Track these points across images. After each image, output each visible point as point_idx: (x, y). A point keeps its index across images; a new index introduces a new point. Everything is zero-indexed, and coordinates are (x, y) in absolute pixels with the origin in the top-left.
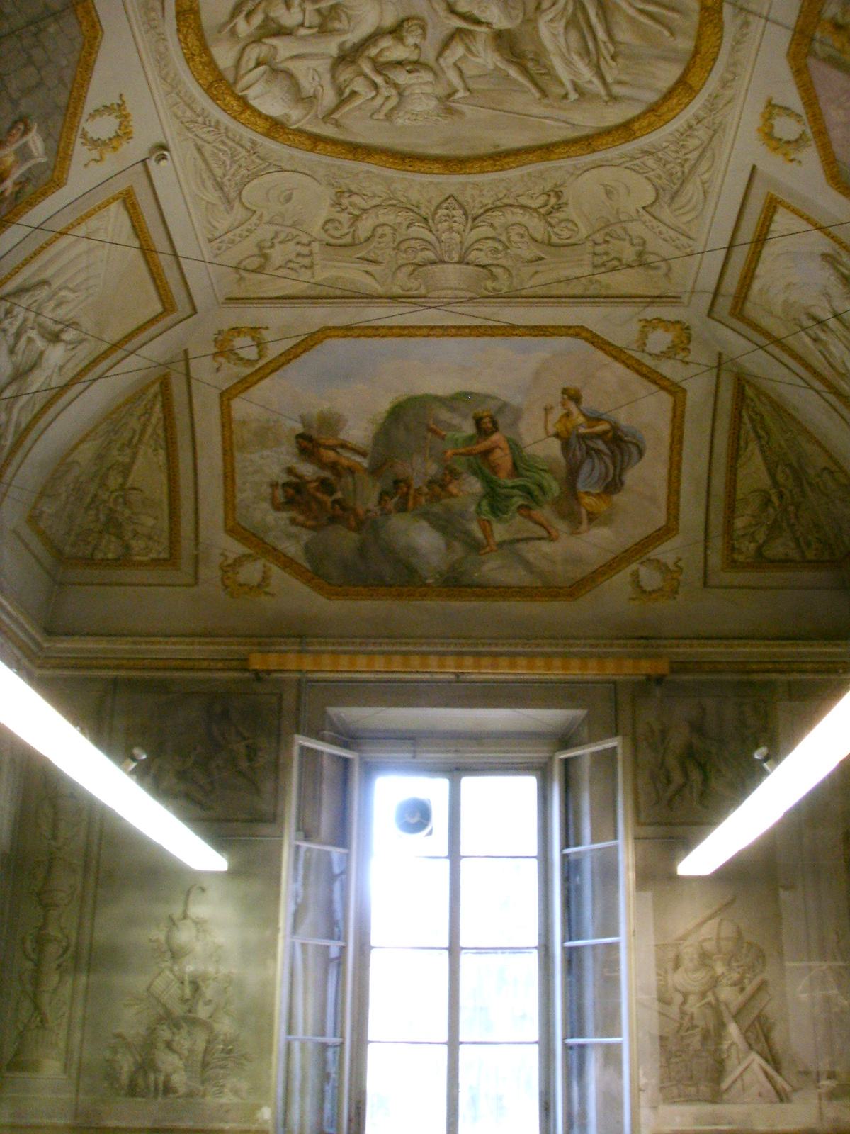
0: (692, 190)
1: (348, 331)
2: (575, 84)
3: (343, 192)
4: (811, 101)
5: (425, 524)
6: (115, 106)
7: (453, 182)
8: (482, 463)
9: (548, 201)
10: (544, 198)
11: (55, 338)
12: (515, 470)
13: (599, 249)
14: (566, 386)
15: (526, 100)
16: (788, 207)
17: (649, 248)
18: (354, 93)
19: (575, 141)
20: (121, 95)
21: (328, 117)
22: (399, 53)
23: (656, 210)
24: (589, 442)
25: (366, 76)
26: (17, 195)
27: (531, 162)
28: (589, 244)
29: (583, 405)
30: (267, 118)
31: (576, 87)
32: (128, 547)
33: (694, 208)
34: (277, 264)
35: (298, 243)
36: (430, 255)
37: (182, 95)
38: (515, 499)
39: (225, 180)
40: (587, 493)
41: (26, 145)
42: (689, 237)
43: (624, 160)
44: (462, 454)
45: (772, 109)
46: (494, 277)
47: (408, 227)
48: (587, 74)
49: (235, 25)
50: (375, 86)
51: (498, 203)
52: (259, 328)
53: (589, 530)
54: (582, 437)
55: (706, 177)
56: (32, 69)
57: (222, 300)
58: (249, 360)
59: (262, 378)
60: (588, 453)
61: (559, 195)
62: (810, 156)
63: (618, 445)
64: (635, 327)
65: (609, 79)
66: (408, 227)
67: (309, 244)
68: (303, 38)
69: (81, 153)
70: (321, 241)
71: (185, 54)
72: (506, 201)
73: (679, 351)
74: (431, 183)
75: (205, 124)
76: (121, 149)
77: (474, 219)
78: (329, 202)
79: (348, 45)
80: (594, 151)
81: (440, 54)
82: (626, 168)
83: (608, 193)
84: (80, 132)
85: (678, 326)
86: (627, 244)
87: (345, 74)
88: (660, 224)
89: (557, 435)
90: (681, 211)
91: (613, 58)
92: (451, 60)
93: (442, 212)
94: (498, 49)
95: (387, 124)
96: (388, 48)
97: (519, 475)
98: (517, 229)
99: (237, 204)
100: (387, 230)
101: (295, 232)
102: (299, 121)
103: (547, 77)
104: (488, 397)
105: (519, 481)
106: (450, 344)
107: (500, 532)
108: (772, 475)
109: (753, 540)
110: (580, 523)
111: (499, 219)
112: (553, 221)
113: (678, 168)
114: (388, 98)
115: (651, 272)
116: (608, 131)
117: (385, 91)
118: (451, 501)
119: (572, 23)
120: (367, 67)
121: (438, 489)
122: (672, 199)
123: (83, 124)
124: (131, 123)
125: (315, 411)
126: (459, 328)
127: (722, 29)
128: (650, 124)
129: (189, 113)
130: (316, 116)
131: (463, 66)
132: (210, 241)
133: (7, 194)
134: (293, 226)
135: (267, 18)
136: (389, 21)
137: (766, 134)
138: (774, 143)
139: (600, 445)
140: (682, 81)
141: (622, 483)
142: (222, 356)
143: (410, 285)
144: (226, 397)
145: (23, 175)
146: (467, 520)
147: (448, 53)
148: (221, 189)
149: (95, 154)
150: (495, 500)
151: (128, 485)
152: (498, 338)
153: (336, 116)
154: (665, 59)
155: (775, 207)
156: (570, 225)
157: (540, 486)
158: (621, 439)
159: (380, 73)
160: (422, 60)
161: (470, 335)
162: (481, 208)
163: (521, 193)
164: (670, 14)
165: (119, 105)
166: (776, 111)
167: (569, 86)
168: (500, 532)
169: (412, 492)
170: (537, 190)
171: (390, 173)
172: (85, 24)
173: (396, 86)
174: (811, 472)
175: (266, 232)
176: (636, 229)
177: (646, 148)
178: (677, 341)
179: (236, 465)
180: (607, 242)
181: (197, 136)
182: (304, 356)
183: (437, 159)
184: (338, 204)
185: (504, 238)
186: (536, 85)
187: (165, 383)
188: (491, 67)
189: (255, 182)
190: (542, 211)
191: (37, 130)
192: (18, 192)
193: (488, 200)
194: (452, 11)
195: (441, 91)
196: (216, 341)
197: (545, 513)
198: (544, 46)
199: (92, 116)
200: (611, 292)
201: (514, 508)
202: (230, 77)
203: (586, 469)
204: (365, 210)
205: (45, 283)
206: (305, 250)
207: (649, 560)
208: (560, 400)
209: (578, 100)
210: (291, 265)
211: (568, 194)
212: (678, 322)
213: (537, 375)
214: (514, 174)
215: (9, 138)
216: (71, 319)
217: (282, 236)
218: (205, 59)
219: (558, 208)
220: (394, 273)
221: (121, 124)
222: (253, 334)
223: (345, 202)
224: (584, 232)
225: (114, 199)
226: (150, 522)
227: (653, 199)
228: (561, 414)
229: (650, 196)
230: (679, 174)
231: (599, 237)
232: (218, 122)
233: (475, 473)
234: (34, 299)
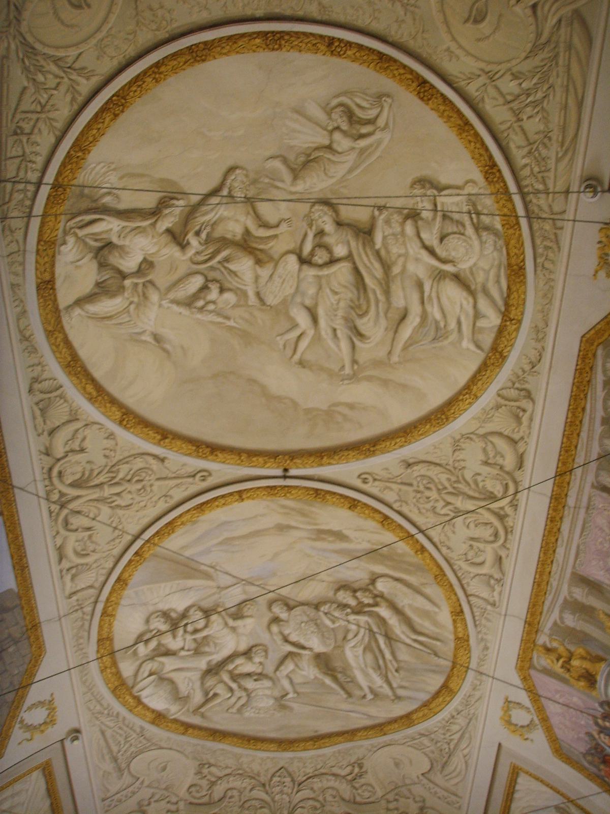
0: (457, 761)
2: (370, 688)
3: (204, 764)
7: (284, 757)
9: (353, 770)
10: (349, 769)
13: (391, 806)
15: (336, 699)
16: (527, 773)
17: (428, 804)
18: (216, 695)
19: (373, 727)
21: (196, 711)
22: (248, 668)
23: (431, 776)
25: (225, 684)
27: (340, 743)
28: (383, 802)
30: (153, 711)
31: (372, 690)
33: (460, 773)
35: (168, 802)
42: (456, 795)
45: (509, 704)
47: (251, 790)
48: (378, 681)
49: (136, 649)
50: (231, 690)
51: (316, 773)
55: (466, 752)
61: (361, 766)
65: (395, 685)
66: (251, 790)
67: (177, 803)
68: (183, 657)
70: (186, 800)
71: (100, 667)
72: (323, 771)
74: (268, 758)
76: (46, 732)
77: (300, 784)
78: (193, 771)
79: (214, 662)
80: (385, 734)
81: (277, 669)
82: (409, 746)
83: (397, 765)
86: (411, 801)
87: (210, 682)
91: (397, 671)
92: (285, 673)
93: (276, 779)
94: (318, 666)
95: (237, 716)
96: (241, 664)
98: (330, 792)
99: (126, 772)
100: (235, 793)
101: (166, 794)
102: (175, 714)
103: (350, 684)
111: (317, 784)
112: (357, 785)
113: (446, 746)
114: (240, 698)
116: (394, 721)
117: (238, 693)
119: (367, 649)
120: (226, 677)
122: (443, 767)
127: (470, 651)
129: (98, 707)
130: (188, 710)
131: (292, 676)
132: (103, 800)
134: (166, 789)
135: (159, 645)
136: (243, 647)
137: (506, 721)
138: (512, 728)
140: (445, 686)
147: (282, 668)
149: (27, 735)
153: (202, 710)
154: (434, 671)
155: (518, 774)
156: (370, 788)
159: (235, 681)
160: (264, 672)
164: (435, 642)
166: (511, 705)
167: (367, 691)
170: (345, 763)
171: (238, 750)
173: (246, 690)
175: (145, 793)
176: (418, 790)
177: (422, 732)
180: (396, 800)
181: (102, 723)
183: (272, 741)
184: (199, 773)
185: (321, 798)
186: (343, 688)
188: (312, 677)
189: (140, 756)
190: (349, 778)
193: (310, 770)
194: (286, 640)
195: (277, 693)
198: (349, 665)
199: (30, 709)
202: (130, 682)
204: (220, 778)
209: (373, 699)
211: (367, 765)
214: (328, 751)
217: (156, 798)
218: (114, 670)
219: (360, 776)
221: (49, 714)
223: (205, 771)
224: (380, 793)
225: (36, 768)
227: (429, 768)
229: (426, 766)
230: (447, 750)
231: (391, 797)
232: (118, 714)
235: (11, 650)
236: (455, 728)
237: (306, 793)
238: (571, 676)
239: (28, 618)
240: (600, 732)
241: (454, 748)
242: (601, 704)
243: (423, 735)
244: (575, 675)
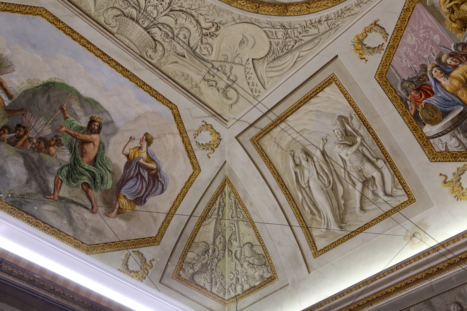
1: (55, 21)
4: (400, 29)
5: (21, 161)
8: (78, 146)
12: (94, 162)
14: (149, 132)
24: (141, 169)
29: (150, 148)
36: (134, 13)
38: (84, 177)
40: (125, 197)
43: (267, 26)
44: (71, 135)
46: (155, 50)
51: (189, 11)
53: (115, 218)
54: (139, 165)
60: (137, 175)
62: (375, 60)
63: (154, 179)
64: (199, 123)
72: (193, 13)
73: (210, 149)
77: (171, 10)
83: (242, 42)
85: (217, 136)
88: (253, 72)
89: (128, 156)
90: (273, 69)
97: (94, 165)
98: (185, 32)
104: (106, 111)
105: (92, 169)
106: (106, 68)
107: (65, 191)
108: (215, 238)
109: (192, 268)
110: (112, 211)
111: (182, 20)
112: (204, 41)
113: (293, 43)
115: (225, 100)
118: (46, 157)
121: (42, 145)
126: (118, 64)
128: (299, 11)
139: (146, 174)
141: (145, 202)
143: (110, 21)
146: (49, 173)
150: (72, 172)
152: (133, 84)
156: (210, 49)
157: (102, 178)
158: (157, 177)
161: (121, 72)
162: (179, 7)
163: (203, 14)
168: (65, 191)
169: (26, 137)
170: (211, 18)
174: (235, 244)
176: (238, 71)
177: (285, 24)
178: (212, 143)
182: (17, 15)
185: (176, 32)
190: (204, 31)
197: (96, 195)
200: (201, 98)
201: (81, 182)
203: (131, 183)
207: (138, 251)
208: (141, 137)
212: (218, 134)
213: (138, 117)
219: (212, 35)
220: (107, 9)
224: (212, 58)
228: (136, 146)
230: (290, 47)
231: (217, 65)
233: (71, 149)
236: (313, 31)
237: (170, 20)
238: (450, 17)
240: (436, 66)
241: (296, 48)
242: (456, 46)
243: (284, 27)
244: (455, 16)
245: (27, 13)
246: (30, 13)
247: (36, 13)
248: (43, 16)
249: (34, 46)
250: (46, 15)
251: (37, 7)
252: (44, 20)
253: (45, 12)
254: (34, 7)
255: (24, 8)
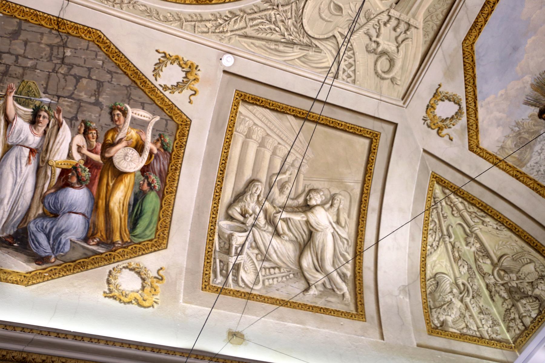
1: (477, 27)
6: (162, 59)
11: (307, 207)
20: (157, 51)
26: (164, 147)
32: (537, 298)
34: (394, 48)
35: (385, 24)
37: (190, 19)
39: (287, 37)
41: (133, 119)
52: (437, 90)
56: (84, 81)
57: (401, 103)
58: (456, 113)
59: (476, 111)
69: (179, 99)
70: (391, 7)
75: (226, 21)
84: (161, 89)
123: (157, 84)
124: (185, 59)
125: (528, 90)
129: (209, 25)
133: (155, 151)
142: (442, 130)
144: (475, 148)
145: (153, 136)
148: (295, 44)
149: (187, 92)
151: (496, 260)
165: (165, 57)
172: (83, 35)
179: (532, 176)
181: (232, 31)
182: (477, 71)
187: (438, 180)
189: (305, 21)
191: (131, 108)
192: (162, 146)
196: (429, 126)
205: (252, 182)
206: (393, 22)
210: (400, 39)
215: (118, 123)
216: (304, 190)
217: (373, 33)
221: (180, 65)
222: (439, 98)
225: (236, 105)
226: (531, 267)
234: (256, 195)
235: (68, 53)
239: (43, 23)
245: (473, 61)
246: (472, 58)
247: (470, 51)
248: (473, 43)
249: (515, 49)
250: (471, 40)
251: (463, 50)
252: (479, 41)
253: (468, 41)
254: (464, 54)
255: (467, 65)
